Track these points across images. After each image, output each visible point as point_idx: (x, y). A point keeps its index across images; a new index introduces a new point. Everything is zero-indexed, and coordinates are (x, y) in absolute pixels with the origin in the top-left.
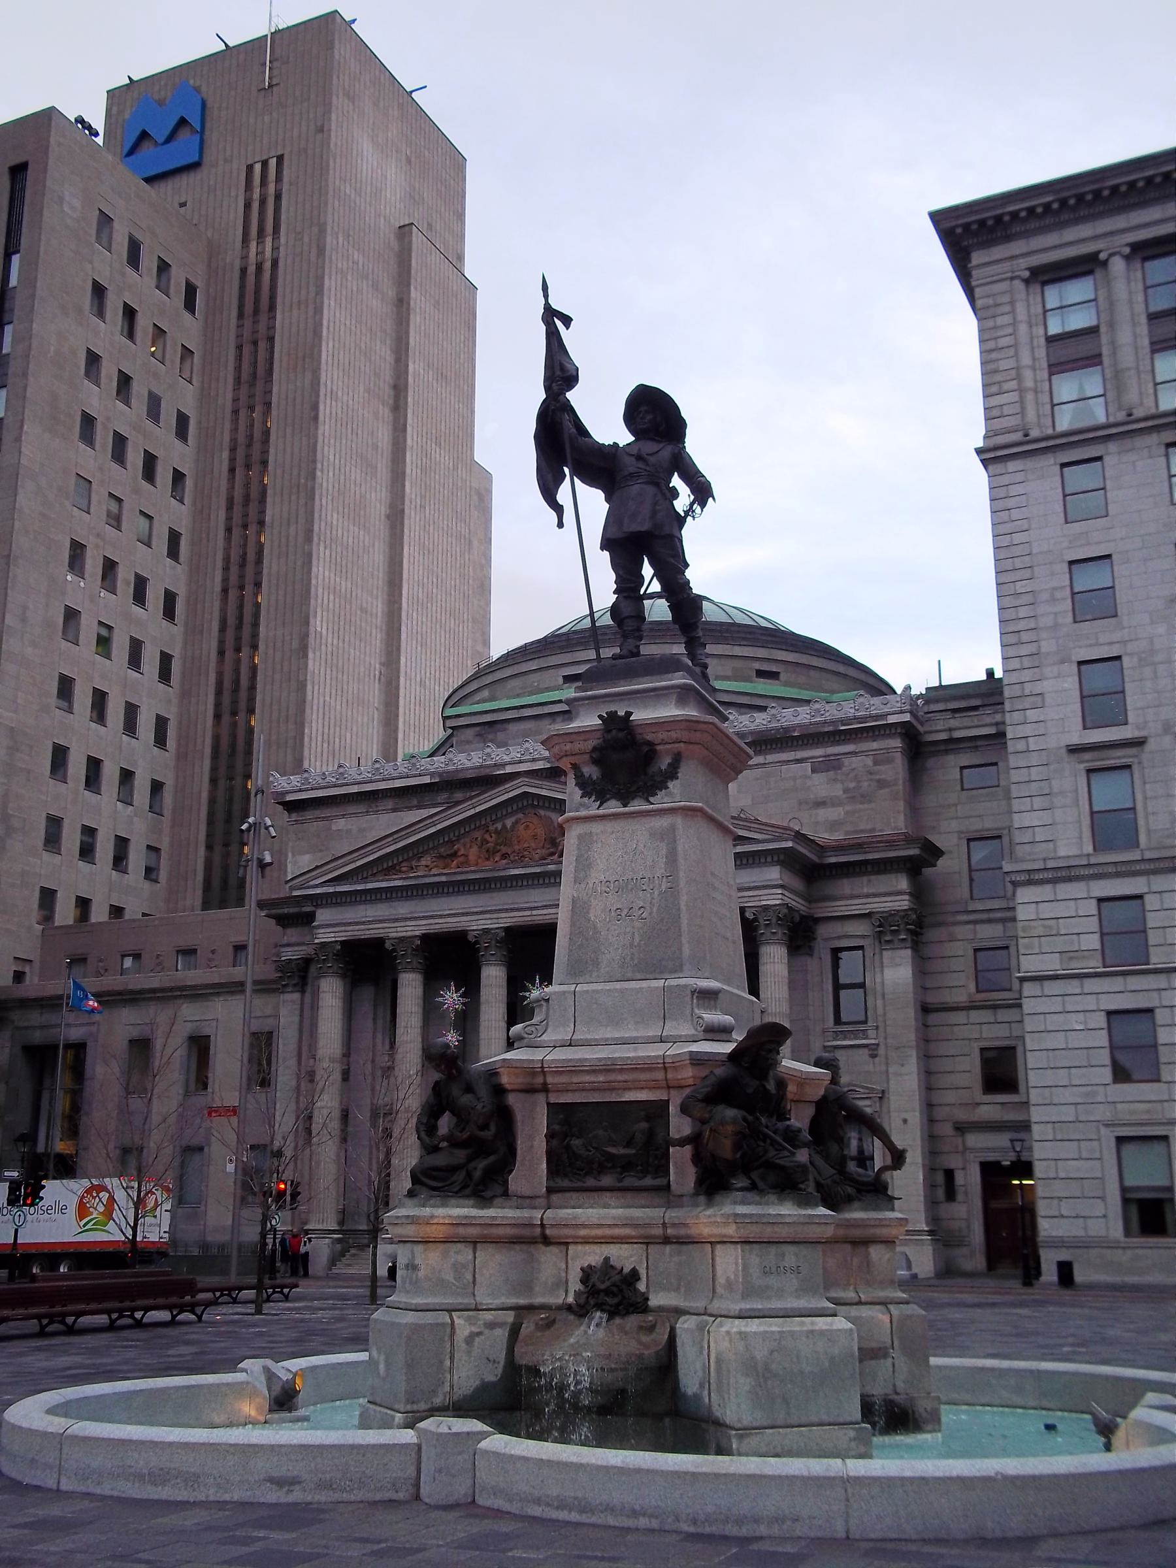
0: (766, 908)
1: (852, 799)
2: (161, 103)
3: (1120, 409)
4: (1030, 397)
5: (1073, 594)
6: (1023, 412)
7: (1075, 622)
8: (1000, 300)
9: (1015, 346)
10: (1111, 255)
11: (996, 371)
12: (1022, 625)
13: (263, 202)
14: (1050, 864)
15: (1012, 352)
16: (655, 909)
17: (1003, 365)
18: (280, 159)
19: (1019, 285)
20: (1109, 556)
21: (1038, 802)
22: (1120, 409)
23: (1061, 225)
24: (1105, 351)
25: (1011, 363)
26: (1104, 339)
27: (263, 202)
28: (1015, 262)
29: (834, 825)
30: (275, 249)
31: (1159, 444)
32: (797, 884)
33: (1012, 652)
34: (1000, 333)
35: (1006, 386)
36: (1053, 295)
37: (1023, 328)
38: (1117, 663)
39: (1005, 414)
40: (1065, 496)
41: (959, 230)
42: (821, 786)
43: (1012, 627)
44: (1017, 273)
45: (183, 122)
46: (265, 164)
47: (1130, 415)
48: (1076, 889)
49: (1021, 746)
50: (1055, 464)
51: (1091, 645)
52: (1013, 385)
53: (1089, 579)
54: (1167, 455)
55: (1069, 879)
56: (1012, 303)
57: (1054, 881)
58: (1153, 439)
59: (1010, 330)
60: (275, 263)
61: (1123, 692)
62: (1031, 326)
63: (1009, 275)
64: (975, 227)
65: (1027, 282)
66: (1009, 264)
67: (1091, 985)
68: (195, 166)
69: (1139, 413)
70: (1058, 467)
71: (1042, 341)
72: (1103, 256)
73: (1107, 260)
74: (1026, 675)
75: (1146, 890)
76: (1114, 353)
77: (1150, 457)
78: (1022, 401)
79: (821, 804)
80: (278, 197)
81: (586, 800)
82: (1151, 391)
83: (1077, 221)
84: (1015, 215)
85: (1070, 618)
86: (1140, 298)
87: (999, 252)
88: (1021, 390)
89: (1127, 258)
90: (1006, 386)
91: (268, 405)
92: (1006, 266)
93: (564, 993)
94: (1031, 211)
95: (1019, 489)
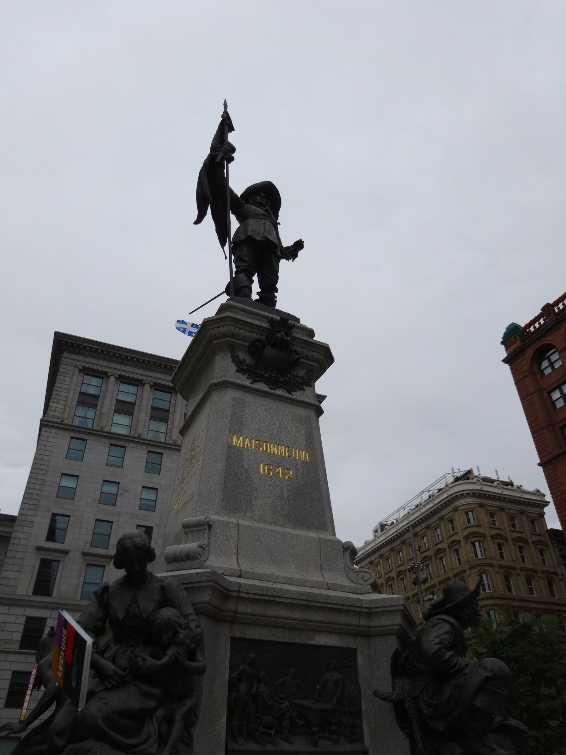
3: (98, 426)
4: (68, 409)
5: (59, 486)
6: (63, 413)
7: (56, 497)
8: (69, 372)
9: (69, 389)
10: (111, 375)
11: (59, 395)
12: (35, 492)
14: (12, 597)
15: (67, 390)
16: (299, 473)
17: (62, 394)
19: (77, 369)
20: (78, 476)
21: (15, 568)
22: (98, 426)
23: (97, 358)
24: (99, 405)
25: (65, 395)
26: (100, 401)
28: (78, 362)
31: (109, 443)
33: (27, 501)
34: (65, 383)
35: (60, 402)
36: (87, 379)
37: (73, 385)
38: (67, 519)
39: (56, 411)
40: (69, 448)
41: (63, 342)
43: (30, 491)
44: (78, 366)
47: (102, 429)
48: (19, 611)
49: (16, 541)
50: (69, 436)
51: (60, 508)
52: (63, 402)
53: (69, 483)
54: (110, 448)
55: (18, 605)
56: (73, 375)
57: (10, 605)
58: (107, 441)
59: (69, 383)
61: (66, 530)
62: (76, 386)
63: (75, 365)
64: (69, 344)
65: (80, 370)
66: (76, 362)
67: (11, 657)
69: (105, 430)
70: (70, 437)
71: (78, 392)
72: (108, 374)
73: (110, 376)
74: (30, 513)
75: (49, 616)
76: (102, 407)
77: (104, 446)
78: (64, 409)
81: (240, 375)
82: (111, 424)
83: (104, 359)
84: (85, 347)
85: (55, 495)
86: (116, 393)
87: (74, 356)
88: (65, 405)
89: (116, 378)
90: (60, 402)
92: (75, 362)
93: (228, 523)
94: (91, 349)
95: (53, 440)
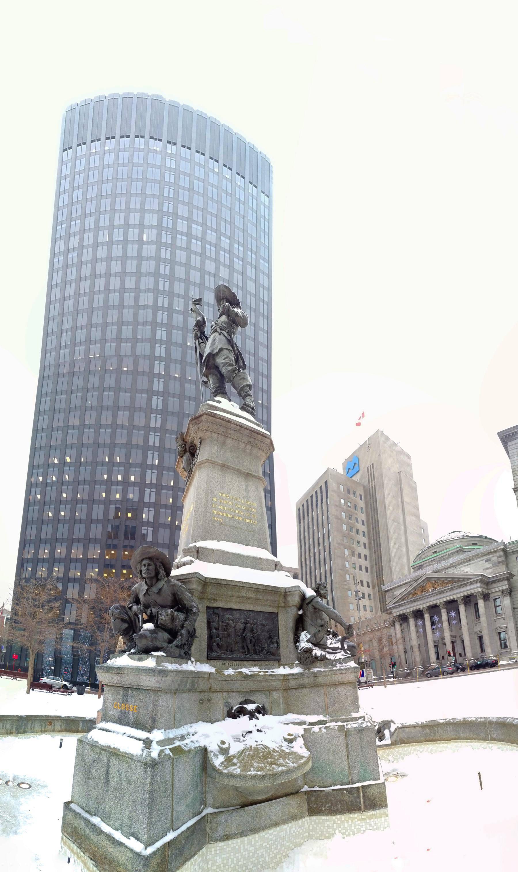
0: (478, 592)
1: (494, 567)
2: (351, 462)
13: (371, 474)
18: (373, 464)
27: (371, 474)
29: (491, 573)
30: (374, 483)
32: (485, 587)
42: (487, 565)
45: (355, 463)
46: (370, 466)
60: (375, 485)
68: (359, 471)
79: (487, 569)
80: (373, 472)
91: (377, 514)
